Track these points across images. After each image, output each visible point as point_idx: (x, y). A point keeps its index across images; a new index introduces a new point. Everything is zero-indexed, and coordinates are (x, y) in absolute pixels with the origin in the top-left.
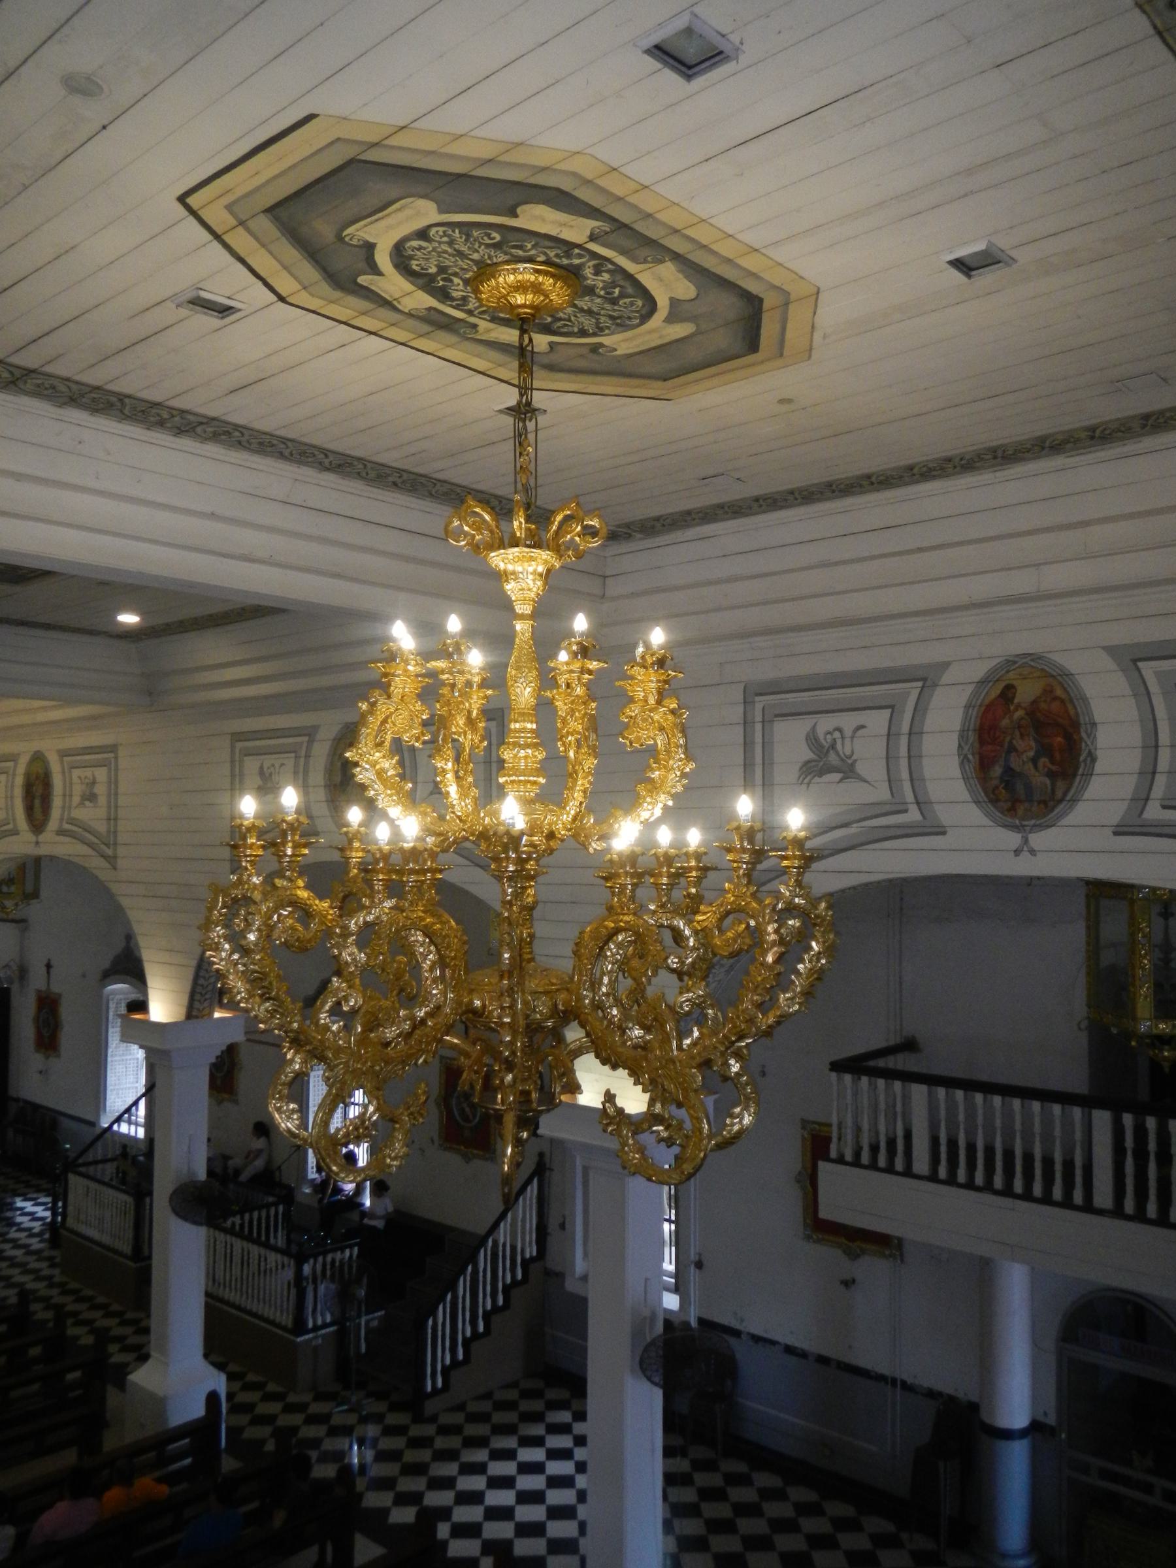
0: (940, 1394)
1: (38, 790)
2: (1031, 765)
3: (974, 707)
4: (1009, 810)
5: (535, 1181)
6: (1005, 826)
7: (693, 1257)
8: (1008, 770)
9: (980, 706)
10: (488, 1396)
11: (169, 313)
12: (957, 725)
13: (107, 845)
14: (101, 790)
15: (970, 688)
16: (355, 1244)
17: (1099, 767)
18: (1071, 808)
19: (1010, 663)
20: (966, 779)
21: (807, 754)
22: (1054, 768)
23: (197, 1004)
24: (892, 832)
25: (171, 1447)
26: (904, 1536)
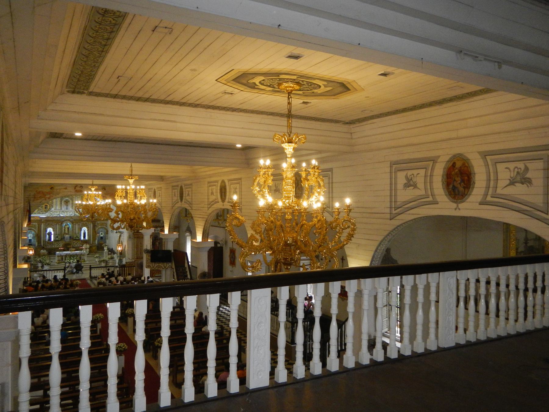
1: (223, 190)
2: (459, 185)
6: (453, 202)
8: (454, 186)
11: (221, 95)
15: (445, 163)
16: (309, 321)
17: (476, 185)
18: (469, 197)
19: (454, 156)
20: (443, 189)
21: (406, 182)
22: (465, 186)
24: (426, 203)
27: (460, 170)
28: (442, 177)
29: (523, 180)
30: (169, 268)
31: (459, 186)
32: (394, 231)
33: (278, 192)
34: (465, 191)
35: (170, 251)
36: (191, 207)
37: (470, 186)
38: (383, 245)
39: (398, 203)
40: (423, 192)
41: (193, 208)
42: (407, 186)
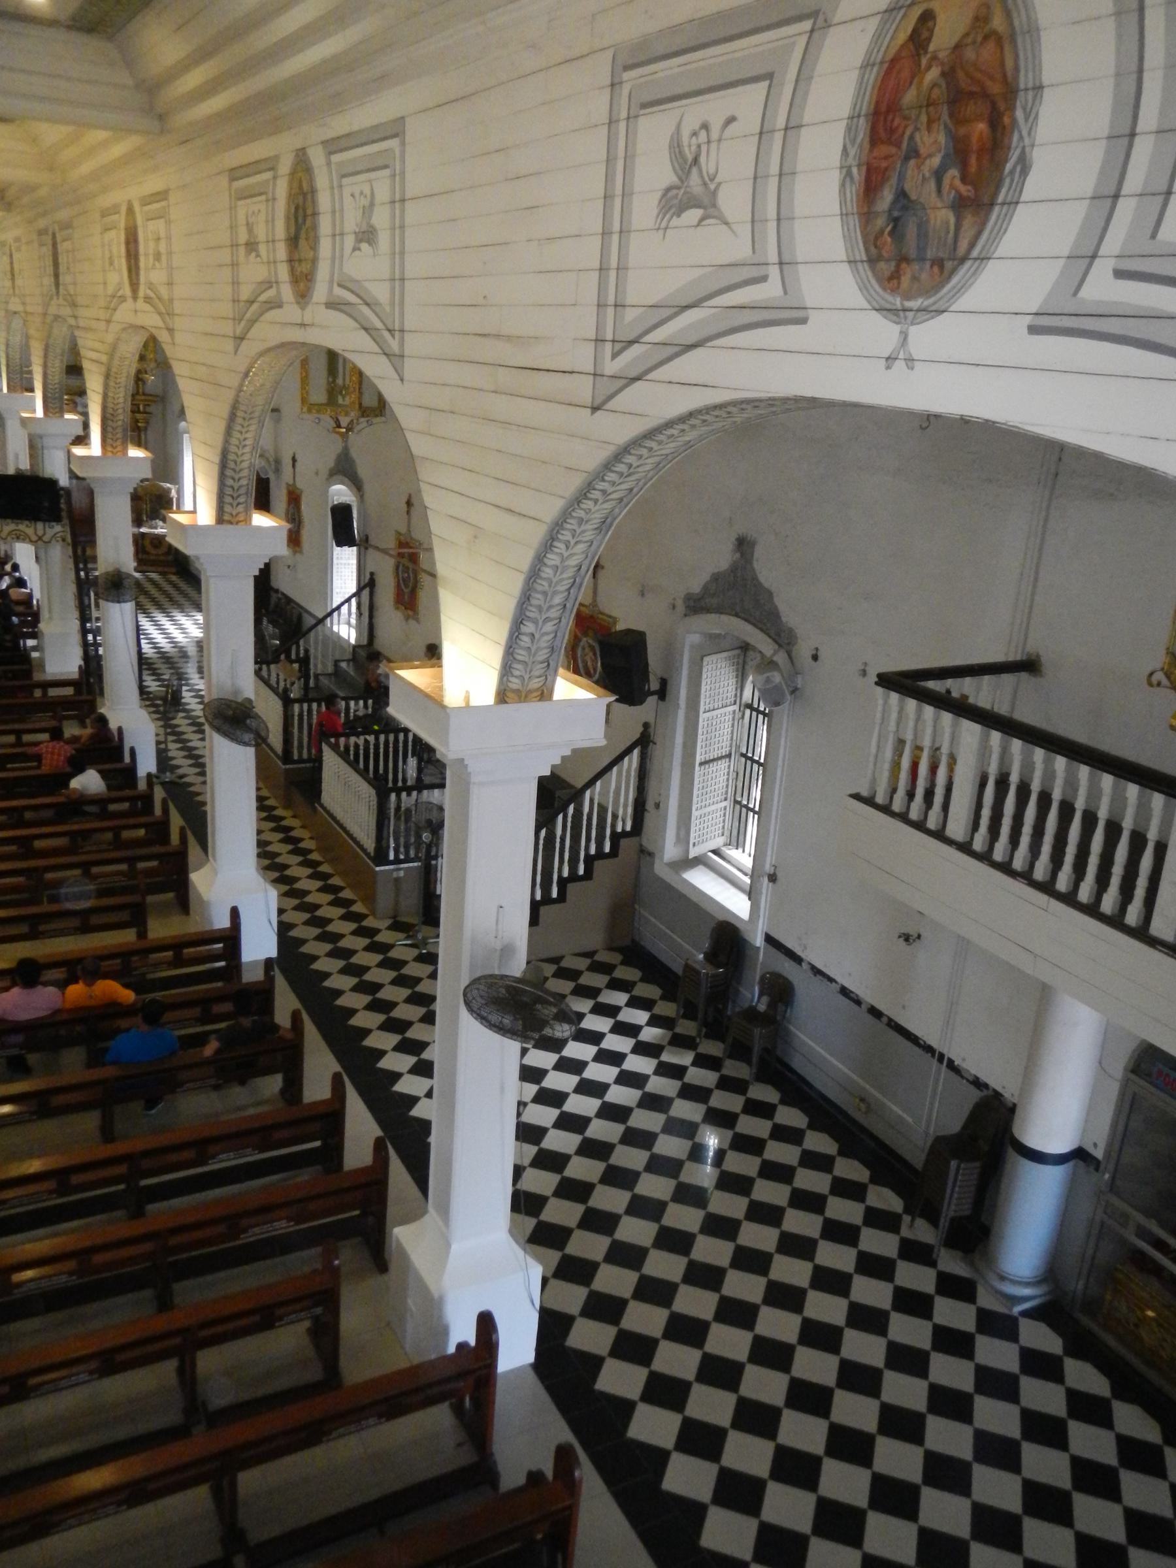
0: (986, 1086)
2: (932, 185)
3: (873, 65)
4: (890, 279)
5: (636, 752)
7: (768, 868)
8: (902, 194)
9: (882, 63)
10: (556, 960)
12: (846, 111)
13: (168, 314)
17: (1033, 186)
21: (670, 178)
22: (965, 190)
23: (227, 508)
25: (186, 951)
26: (907, 1219)
27: (948, 75)
28: (849, 129)
30: (53, 542)
32: (611, 477)
33: (253, 254)
34: (958, 227)
35: (52, 483)
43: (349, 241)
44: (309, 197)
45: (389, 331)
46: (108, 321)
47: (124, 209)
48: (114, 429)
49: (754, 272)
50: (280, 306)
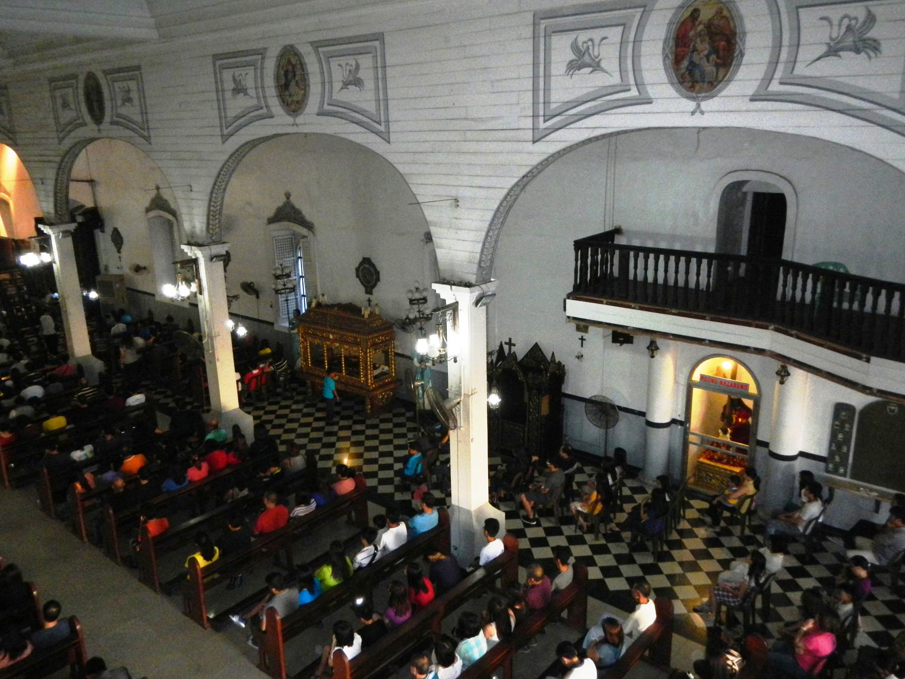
2: (705, 59)
4: (691, 87)
8: (692, 64)
12: (663, 37)
14: (134, 95)
15: (673, 11)
17: (745, 59)
20: (666, 69)
21: (571, 56)
22: (718, 61)
23: (211, 222)
29: (860, 45)
31: (704, 62)
33: (241, 95)
36: (10, 139)
37: (732, 60)
38: (511, 196)
39: (553, 106)
40: (616, 79)
41: (19, 142)
42: (574, 66)
43: (337, 86)
44: (299, 66)
45: (377, 123)
46: (61, 140)
47: (82, 77)
48: (61, 198)
49: (625, 88)
50: (272, 117)
